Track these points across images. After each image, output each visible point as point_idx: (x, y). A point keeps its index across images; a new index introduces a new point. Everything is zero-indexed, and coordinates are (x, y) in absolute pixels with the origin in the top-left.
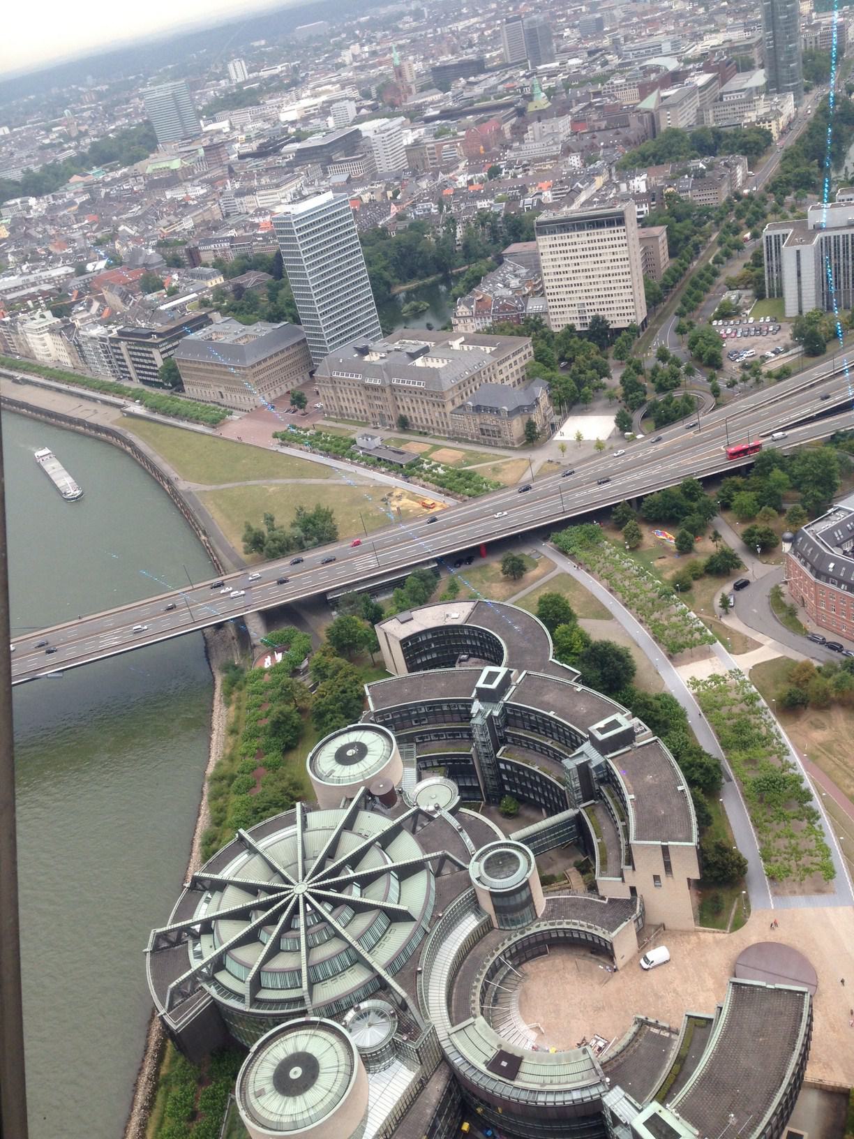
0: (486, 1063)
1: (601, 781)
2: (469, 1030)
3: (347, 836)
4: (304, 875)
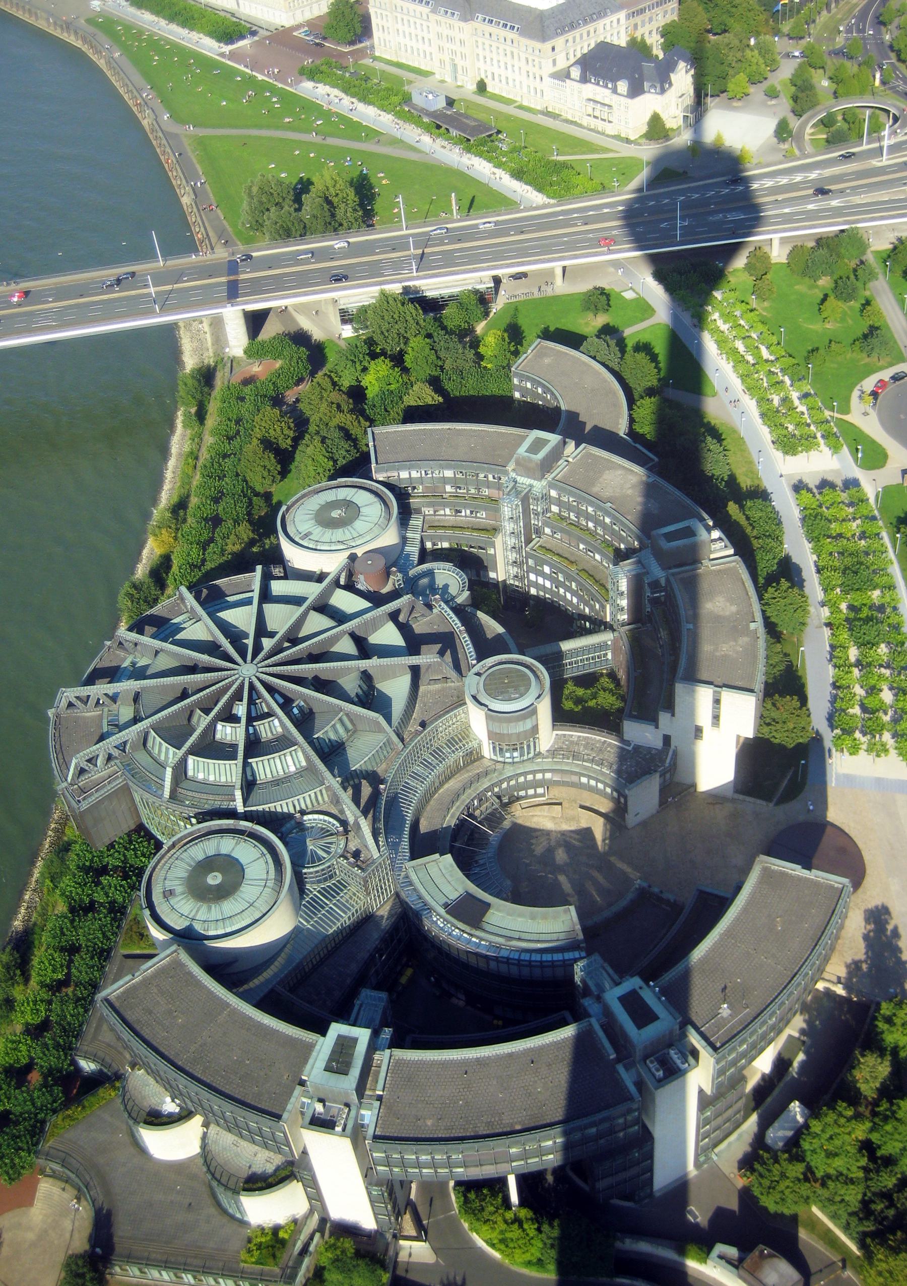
0: (446, 906)
1: (655, 602)
4: (254, 656)
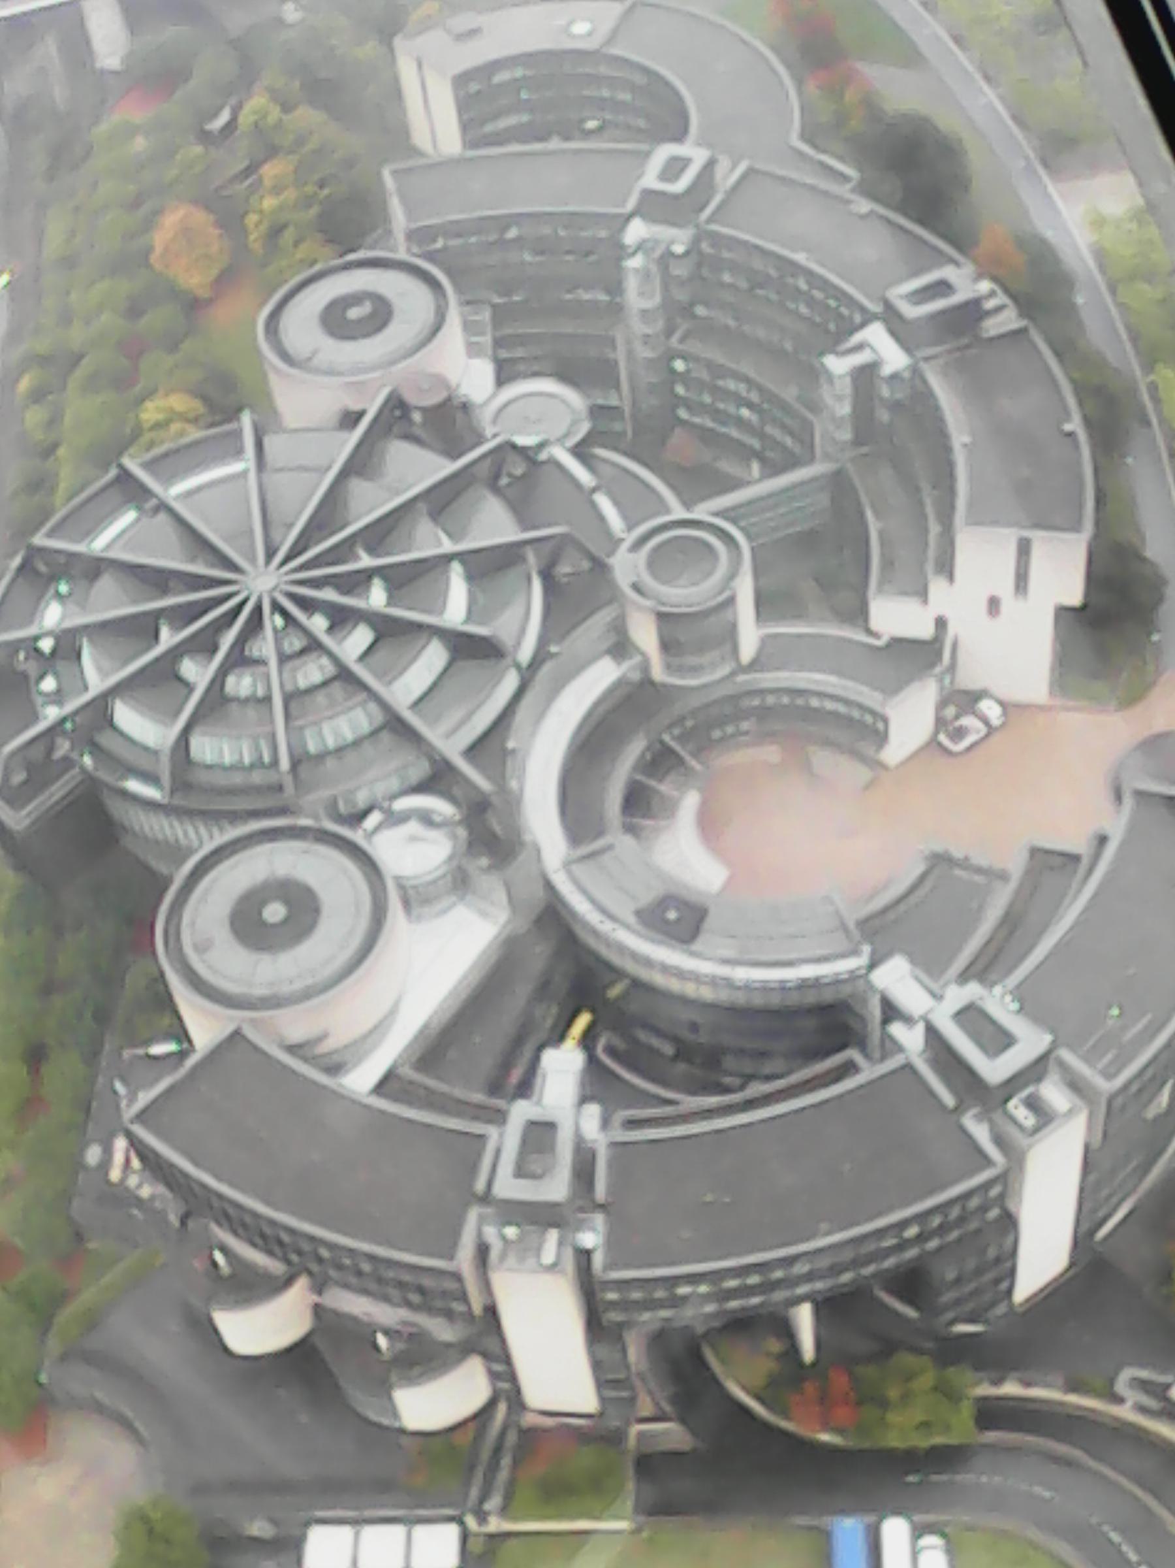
0: (639, 913)
1: (896, 406)
2: (606, 858)
3: (358, 487)
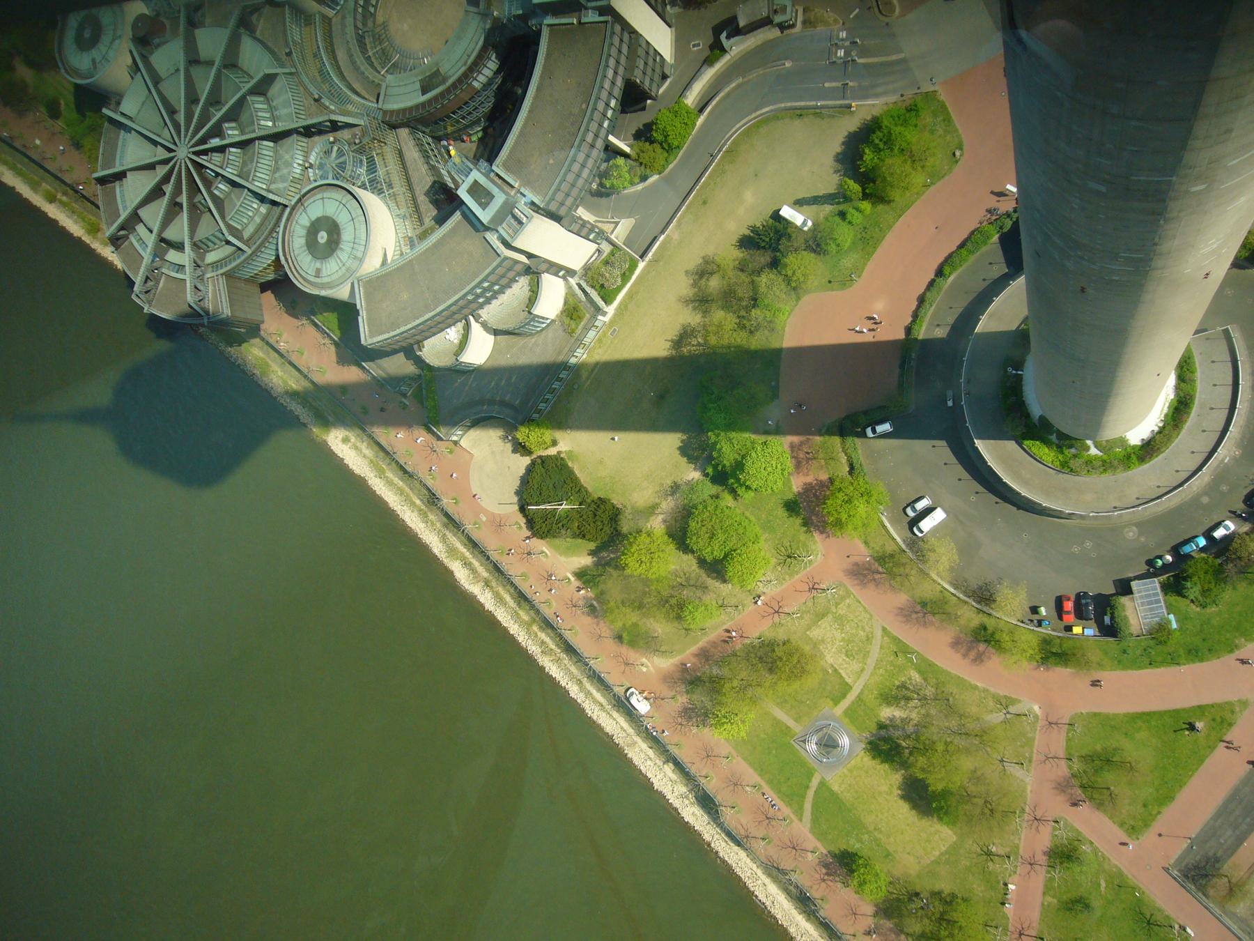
4: (175, 144)
